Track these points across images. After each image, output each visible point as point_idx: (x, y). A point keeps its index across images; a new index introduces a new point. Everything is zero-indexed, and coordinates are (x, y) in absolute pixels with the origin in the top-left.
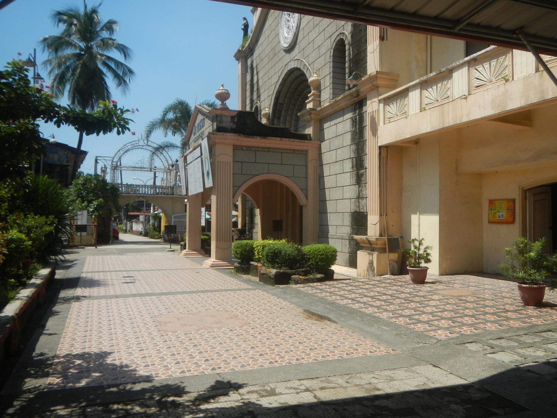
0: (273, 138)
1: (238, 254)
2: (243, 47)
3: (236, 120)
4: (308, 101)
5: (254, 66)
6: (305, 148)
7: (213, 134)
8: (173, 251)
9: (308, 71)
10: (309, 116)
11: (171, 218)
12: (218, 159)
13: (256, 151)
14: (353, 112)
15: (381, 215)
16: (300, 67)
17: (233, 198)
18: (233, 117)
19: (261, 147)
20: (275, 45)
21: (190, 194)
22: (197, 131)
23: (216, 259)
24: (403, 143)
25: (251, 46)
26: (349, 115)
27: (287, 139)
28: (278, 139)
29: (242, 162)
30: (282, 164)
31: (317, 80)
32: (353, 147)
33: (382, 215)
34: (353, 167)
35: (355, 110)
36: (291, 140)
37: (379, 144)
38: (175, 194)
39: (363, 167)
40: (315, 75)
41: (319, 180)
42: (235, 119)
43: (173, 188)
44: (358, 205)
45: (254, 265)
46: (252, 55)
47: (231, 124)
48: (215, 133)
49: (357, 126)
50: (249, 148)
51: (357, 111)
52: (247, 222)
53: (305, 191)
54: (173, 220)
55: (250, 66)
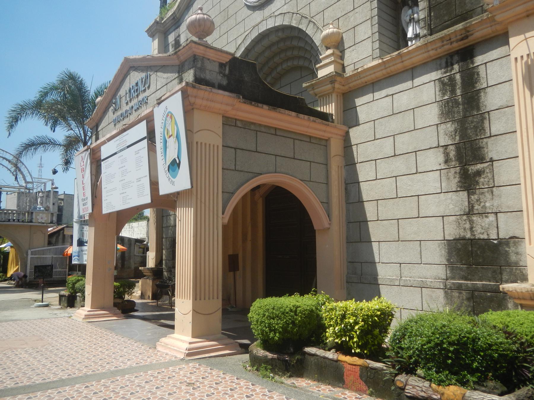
0: (287, 112)
1: (275, 331)
2: (162, 19)
3: (227, 72)
4: (321, 64)
6: (326, 135)
7: (194, 87)
8: (47, 306)
9: (311, 25)
10: (329, 86)
11: (27, 255)
12: (197, 138)
13: (257, 131)
14: (443, 70)
17: (223, 214)
18: (222, 65)
19: (265, 126)
20: (227, 6)
21: (105, 211)
22: (124, 101)
23: (193, 337)
25: (178, 16)
26: (435, 75)
27: (306, 117)
28: (294, 114)
29: (235, 149)
30: (294, 158)
31: (339, 33)
32: (450, 127)
34: (446, 162)
35: (449, 65)
36: (312, 118)
38: (34, 221)
40: (331, 26)
41: (346, 189)
42: (225, 69)
43: (32, 213)
44: (468, 226)
45: (325, 358)
46: (179, 27)
47: (219, 77)
49: (459, 92)
50: (247, 125)
51: (456, 67)
52: (164, 257)
53: (327, 204)
54: (30, 256)
55: (173, 42)
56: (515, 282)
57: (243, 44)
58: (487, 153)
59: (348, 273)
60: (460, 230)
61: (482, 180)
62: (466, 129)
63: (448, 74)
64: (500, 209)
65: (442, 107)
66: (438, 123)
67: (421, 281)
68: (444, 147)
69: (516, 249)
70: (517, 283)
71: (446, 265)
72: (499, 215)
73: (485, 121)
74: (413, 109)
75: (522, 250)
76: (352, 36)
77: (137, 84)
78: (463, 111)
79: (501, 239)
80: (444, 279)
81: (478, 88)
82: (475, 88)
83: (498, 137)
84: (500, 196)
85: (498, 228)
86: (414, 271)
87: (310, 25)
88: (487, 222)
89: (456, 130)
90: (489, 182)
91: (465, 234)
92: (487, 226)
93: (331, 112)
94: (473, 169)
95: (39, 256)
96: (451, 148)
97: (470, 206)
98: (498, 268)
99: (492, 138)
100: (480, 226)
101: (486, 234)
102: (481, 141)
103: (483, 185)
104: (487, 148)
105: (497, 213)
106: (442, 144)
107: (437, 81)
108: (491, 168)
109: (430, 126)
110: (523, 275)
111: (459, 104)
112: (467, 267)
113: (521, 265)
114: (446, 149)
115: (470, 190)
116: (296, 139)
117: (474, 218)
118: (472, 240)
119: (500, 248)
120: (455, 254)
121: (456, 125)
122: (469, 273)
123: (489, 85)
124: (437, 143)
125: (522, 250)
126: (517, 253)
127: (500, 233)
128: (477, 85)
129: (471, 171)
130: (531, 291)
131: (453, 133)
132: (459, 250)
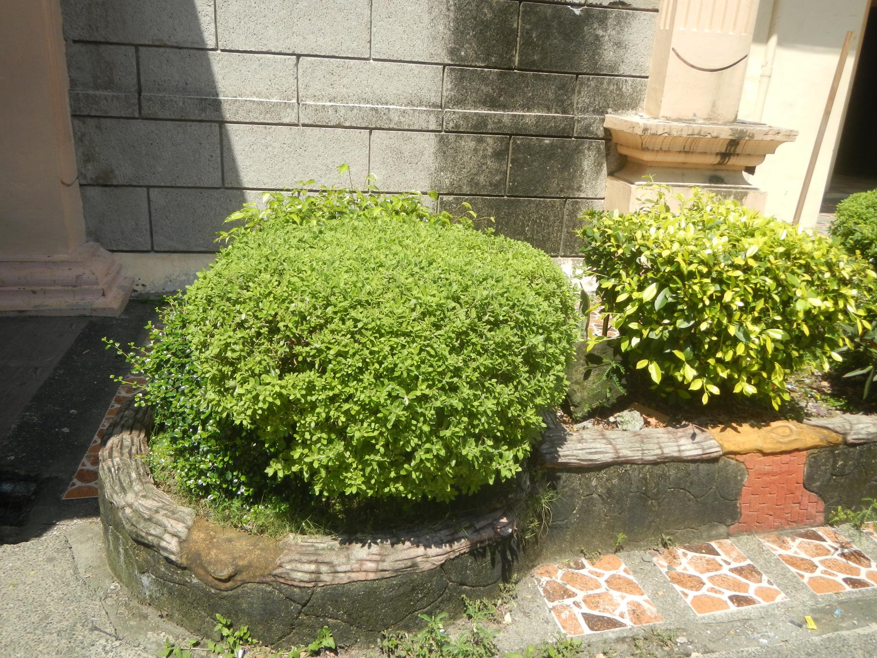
59: (73, 83)
67: (372, 109)
69: (619, 33)
71: (445, 65)
75: (631, 37)
79: (591, 5)
80: (434, 105)
86: (345, 81)
98: (572, 78)
110: (621, 96)
112: (501, 74)
113: (621, 73)
119: (585, 28)
120: (474, 36)
122: (501, 90)
125: (631, 37)
126: (619, 44)
130: (699, 134)
132: (486, 25)
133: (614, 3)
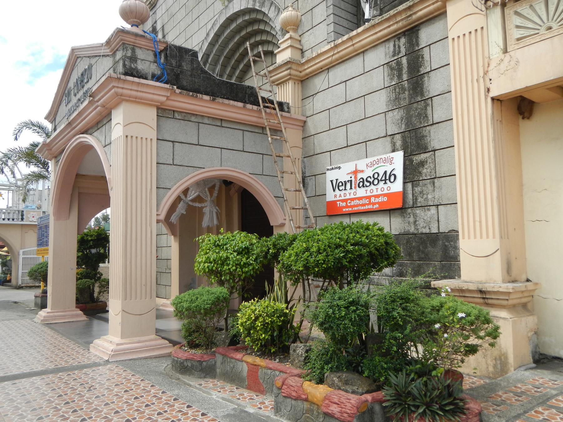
3: (162, 60)
4: (279, 49)
5: (159, 26)
9: (273, 8)
11: (19, 255)
15: (501, 237)
16: (254, 5)
17: (157, 211)
24: (548, 89)
28: (240, 104)
29: (173, 142)
32: (397, 115)
33: (503, 237)
37: (495, 93)
39: (426, 148)
40: (290, 9)
42: (160, 59)
44: (412, 219)
48: (123, 77)
49: (405, 77)
54: (21, 256)
56: (450, 278)
57: (212, 30)
58: (430, 142)
60: (405, 224)
61: (425, 171)
62: (411, 116)
63: (396, 58)
64: (441, 202)
65: (390, 93)
66: (386, 111)
68: (392, 136)
70: (455, 278)
72: (440, 207)
73: (428, 107)
74: (364, 96)
76: (310, 18)
77: (82, 75)
78: (409, 97)
79: (441, 233)
81: (422, 73)
82: (420, 72)
83: (439, 124)
84: (440, 188)
85: (438, 221)
87: (272, 7)
88: (429, 216)
89: (402, 117)
90: (431, 172)
91: (409, 229)
92: (429, 219)
93: (288, 102)
94: (417, 159)
95: (28, 256)
96: (398, 138)
97: (414, 198)
99: (435, 126)
100: (422, 220)
101: (427, 228)
102: (424, 129)
103: (426, 176)
104: (430, 137)
105: (438, 205)
106: (389, 133)
107: (386, 65)
108: (433, 157)
109: (378, 114)
111: (405, 90)
112: (411, 264)
114: (393, 138)
115: (414, 181)
116: (246, 131)
117: (418, 212)
118: (415, 234)
121: (402, 113)
123: (432, 69)
124: (385, 133)
127: (440, 227)
128: (421, 69)
129: (415, 161)
131: (400, 121)
133: (450, 231)
